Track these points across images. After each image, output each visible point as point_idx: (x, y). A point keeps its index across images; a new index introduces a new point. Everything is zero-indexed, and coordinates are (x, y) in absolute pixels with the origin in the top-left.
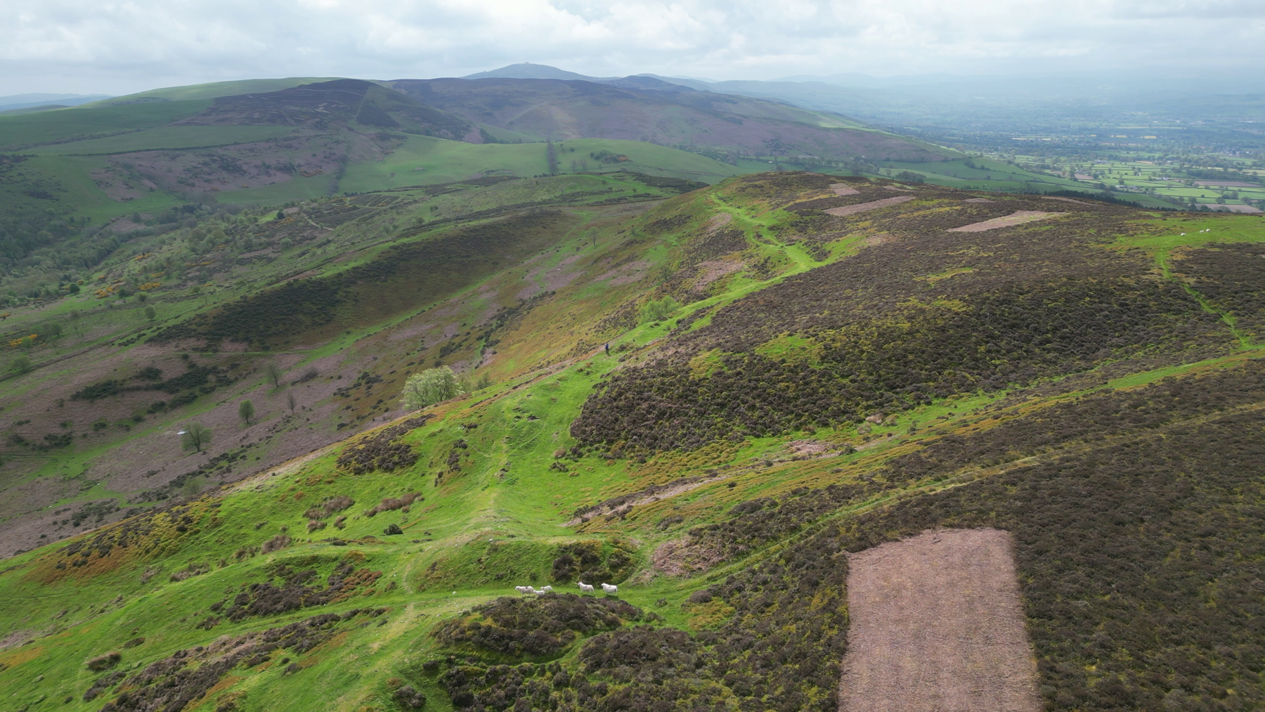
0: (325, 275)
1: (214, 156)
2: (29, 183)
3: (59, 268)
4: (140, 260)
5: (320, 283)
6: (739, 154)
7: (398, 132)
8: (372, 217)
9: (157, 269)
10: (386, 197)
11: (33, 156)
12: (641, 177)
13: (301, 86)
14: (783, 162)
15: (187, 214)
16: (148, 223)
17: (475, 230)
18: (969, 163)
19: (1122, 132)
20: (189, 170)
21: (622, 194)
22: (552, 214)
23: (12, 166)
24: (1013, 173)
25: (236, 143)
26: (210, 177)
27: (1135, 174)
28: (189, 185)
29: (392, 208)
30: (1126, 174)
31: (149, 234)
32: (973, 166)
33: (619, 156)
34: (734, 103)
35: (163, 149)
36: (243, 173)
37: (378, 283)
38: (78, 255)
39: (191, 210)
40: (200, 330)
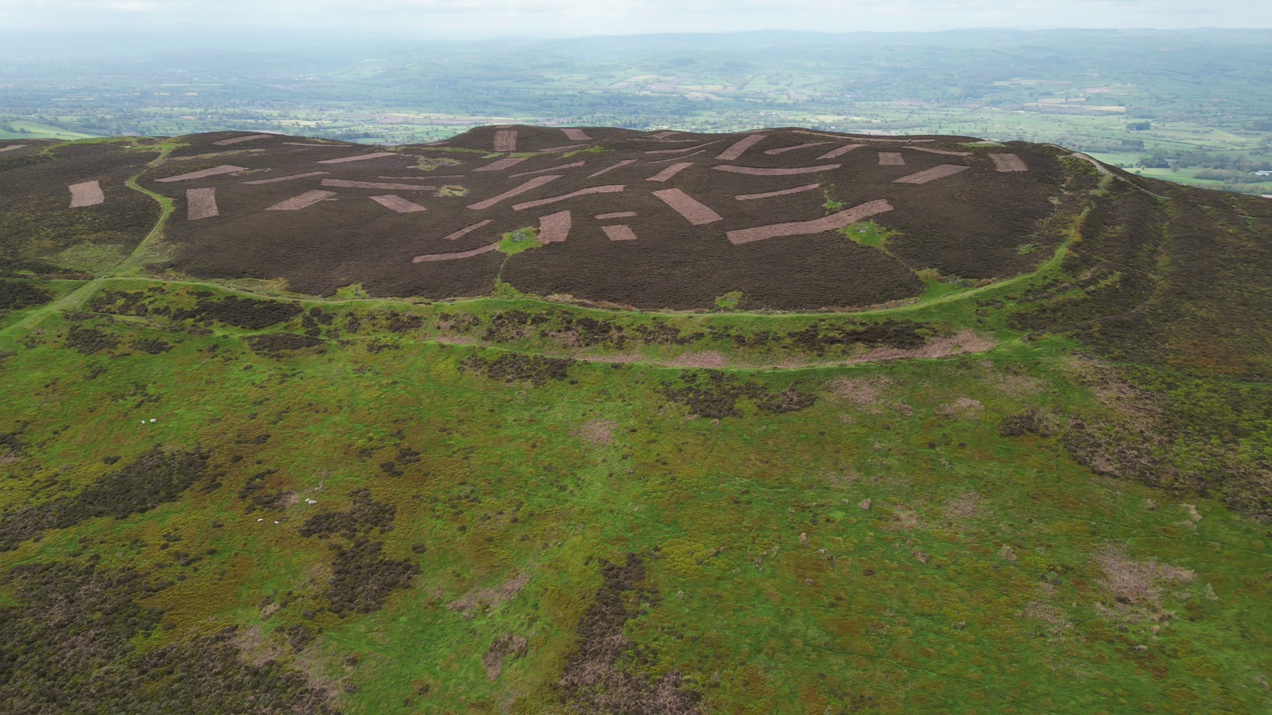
19: (165, 90)
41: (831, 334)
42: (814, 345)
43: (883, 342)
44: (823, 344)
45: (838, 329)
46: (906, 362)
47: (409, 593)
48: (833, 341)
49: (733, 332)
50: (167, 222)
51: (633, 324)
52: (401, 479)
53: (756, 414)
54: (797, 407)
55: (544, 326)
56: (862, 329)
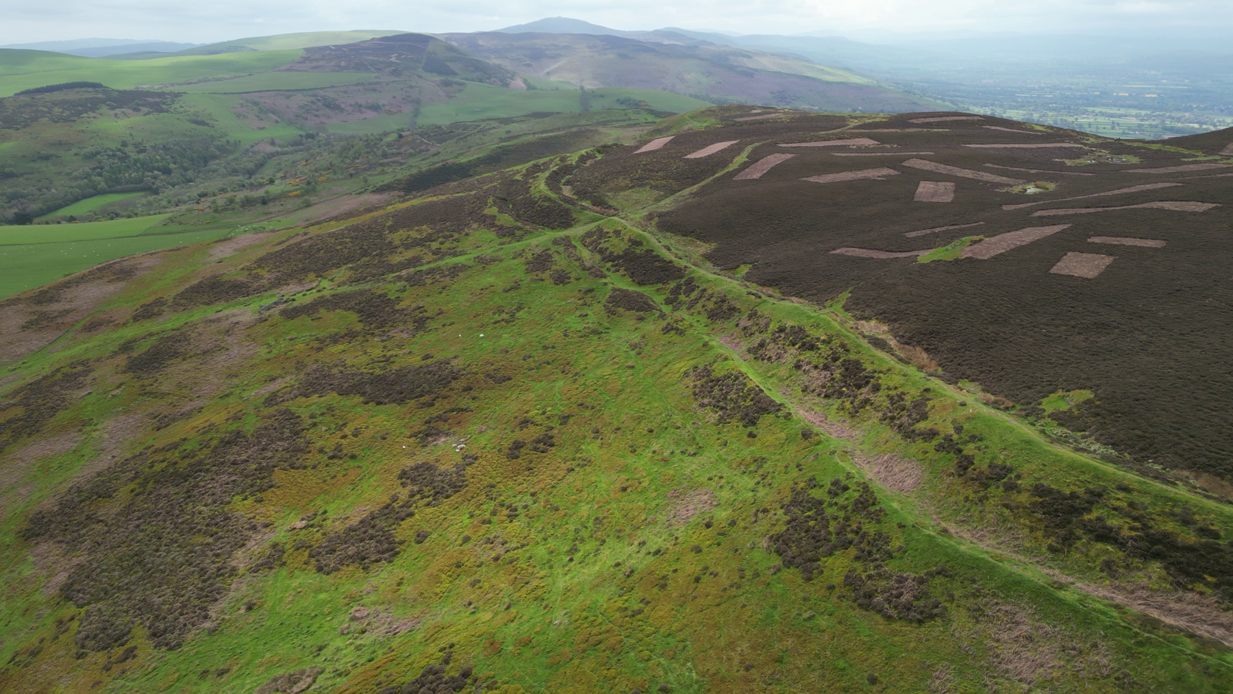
0: (462, 161)
3: (230, 175)
4: (306, 165)
5: (460, 165)
8: (465, 137)
9: (324, 170)
10: (471, 126)
11: (184, 93)
12: (652, 112)
15: (310, 140)
16: (280, 146)
17: (546, 138)
20: (302, 107)
21: (637, 122)
22: (592, 131)
25: (332, 87)
26: (317, 113)
27: (1113, 128)
29: (478, 132)
30: (1104, 128)
31: (286, 153)
33: (640, 101)
34: (749, 57)
36: (342, 110)
38: (242, 166)
39: (312, 136)
40: (399, 187)
41: (1113, 522)
42: (1059, 526)
43: (1216, 586)
44: (1079, 532)
45: (1135, 519)
46: (1190, 646)
47: (360, 573)
48: (1105, 535)
49: (969, 449)
50: (714, 179)
51: (896, 388)
52: (508, 463)
53: (832, 588)
54: (893, 613)
55: (808, 355)
56: (1189, 537)
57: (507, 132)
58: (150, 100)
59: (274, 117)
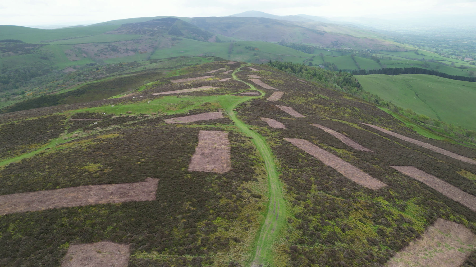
1: (110, 45)
2: (43, 54)
6: (316, 47)
7: (182, 38)
11: (48, 44)
13: (153, 20)
14: (334, 51)
17: (121, 78)
18: (416, 53)
23: (39, 48)
24: (435, 57)
25: (120, 41)
26: (106, 53)
28: (98, 56)
32: (418, 54)
33: (255, 48)
34: (326, 26)
35: (94, 43)
37: (76, 97)
57: (144, 68)
58: (26, 48)
59: (84, 55)
